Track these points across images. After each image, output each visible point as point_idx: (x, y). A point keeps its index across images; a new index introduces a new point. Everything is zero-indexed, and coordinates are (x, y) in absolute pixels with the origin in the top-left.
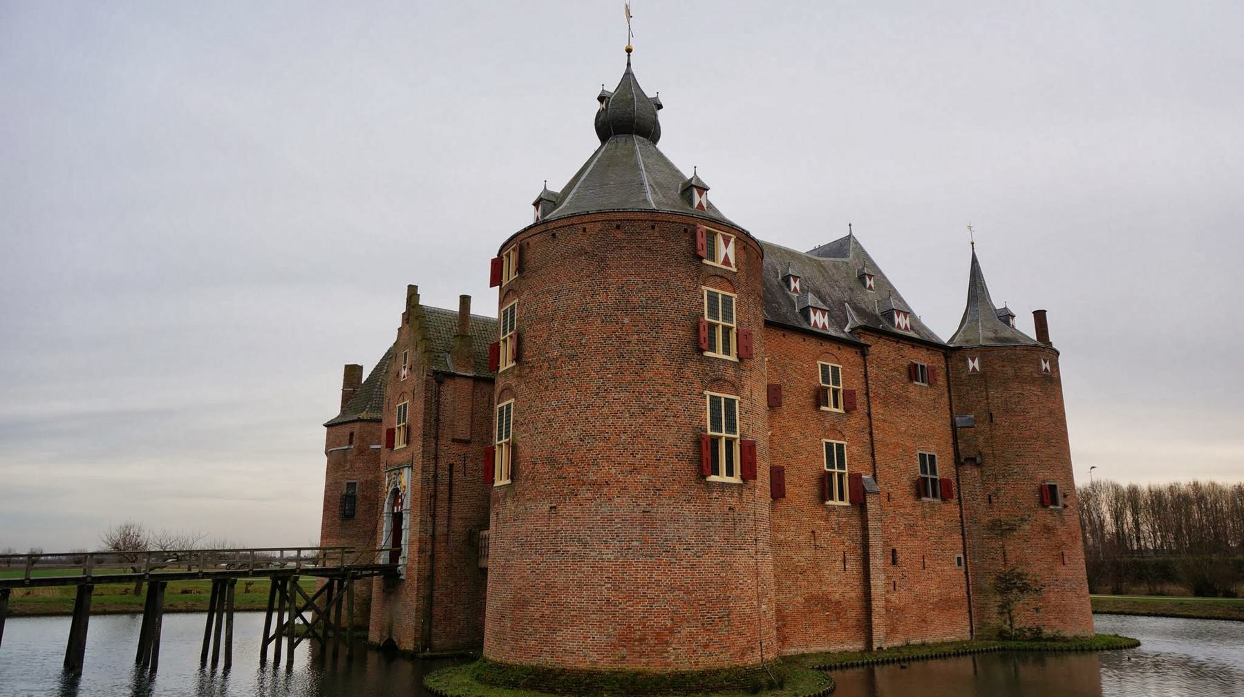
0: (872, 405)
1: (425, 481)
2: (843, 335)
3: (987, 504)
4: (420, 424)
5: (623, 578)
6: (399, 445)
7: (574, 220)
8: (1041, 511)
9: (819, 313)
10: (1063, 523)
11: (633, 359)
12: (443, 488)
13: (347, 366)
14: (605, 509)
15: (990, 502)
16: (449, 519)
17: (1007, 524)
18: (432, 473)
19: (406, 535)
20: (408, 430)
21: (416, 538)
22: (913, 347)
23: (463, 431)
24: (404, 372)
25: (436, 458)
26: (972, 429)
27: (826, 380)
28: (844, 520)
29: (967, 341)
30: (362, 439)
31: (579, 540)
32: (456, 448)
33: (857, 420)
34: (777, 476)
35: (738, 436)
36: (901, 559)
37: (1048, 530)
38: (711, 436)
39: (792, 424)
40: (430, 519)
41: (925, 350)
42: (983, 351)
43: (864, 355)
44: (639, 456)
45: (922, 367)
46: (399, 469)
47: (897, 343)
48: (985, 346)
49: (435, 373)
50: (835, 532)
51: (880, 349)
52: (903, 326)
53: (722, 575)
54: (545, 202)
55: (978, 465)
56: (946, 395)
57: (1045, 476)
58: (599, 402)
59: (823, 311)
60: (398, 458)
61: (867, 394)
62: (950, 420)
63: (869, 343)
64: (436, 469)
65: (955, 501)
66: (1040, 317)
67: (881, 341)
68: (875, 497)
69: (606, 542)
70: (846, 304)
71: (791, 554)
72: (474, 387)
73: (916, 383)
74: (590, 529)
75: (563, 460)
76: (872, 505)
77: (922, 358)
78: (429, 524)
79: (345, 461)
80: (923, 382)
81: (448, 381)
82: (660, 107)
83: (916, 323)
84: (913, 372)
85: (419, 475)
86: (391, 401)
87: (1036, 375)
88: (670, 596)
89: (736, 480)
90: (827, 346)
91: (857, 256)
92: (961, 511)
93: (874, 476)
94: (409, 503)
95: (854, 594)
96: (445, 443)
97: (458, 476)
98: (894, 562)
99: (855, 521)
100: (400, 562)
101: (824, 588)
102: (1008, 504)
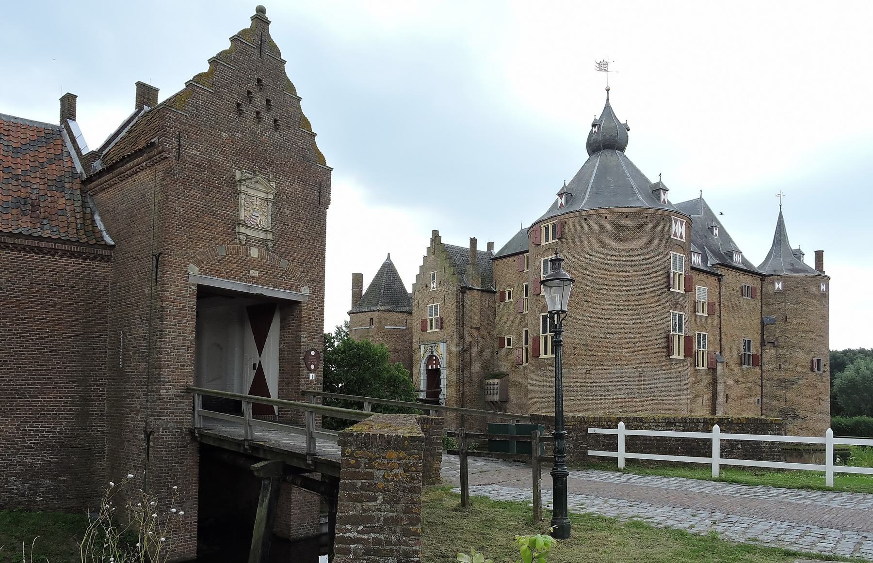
1: (458, 352)
7: (600, 211)
11: (634, 293)
12: (467, 355)
15: (780, 369)
16: (471, 373)
18: (462, 347)
19: (443, 383)
23: (476, 322)
24: (433, 286)
28: (704, 377)
30: (380, 322)
32: (473, 333)
40: (461, 373)
46: (436, 343)
49: (462, 287)
54: (567, 194)
57: (815, 355)
58: (616, 316)
60: (432, 337)
64: (463, 344)
65: (759, 367)
76: (720, 369)
78: (461, 376)
79: (368, 336)
81: (468, 292)
85: (454, 348)
92: (762, 373)
93: (720, 352)
94: (445, 364)
97: (474, 349)
99: (710, 378)
100: (441, 397)
102: (791, 370)
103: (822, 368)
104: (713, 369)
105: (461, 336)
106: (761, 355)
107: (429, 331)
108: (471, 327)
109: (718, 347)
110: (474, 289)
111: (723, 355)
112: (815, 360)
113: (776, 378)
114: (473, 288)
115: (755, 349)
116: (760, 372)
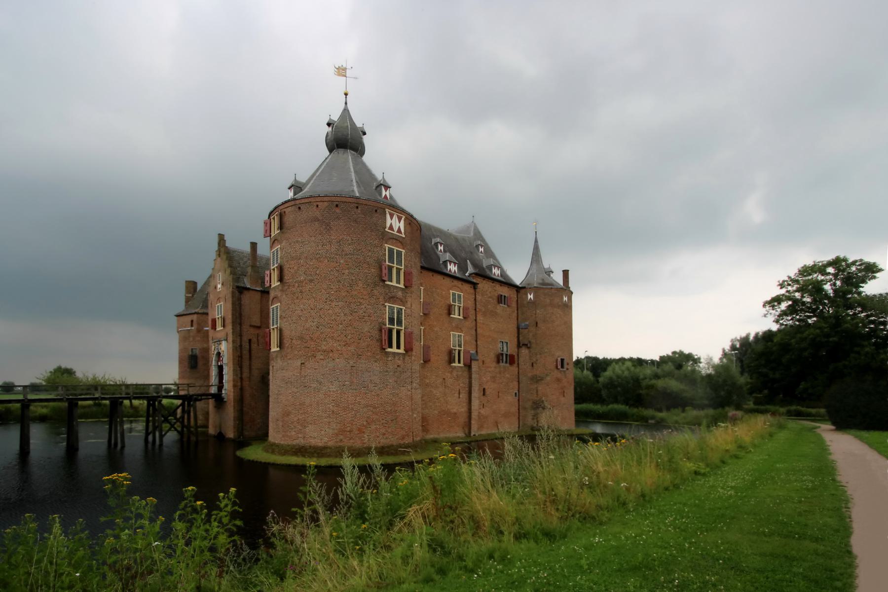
0: (477, 315)
2: (464, 277)
3: (531, 367)
4: (230, 316)
5: (341, 400)
6: (219, 328)
8: (556, 371)
9: (452, 264)
13: (186, 282)
14: (331, 365)
17: (540, 377)
20: (224, 320)
22: (501, 285)
25: (241, 336)
26: (527, 330)
27: (454, 301)
28: (460, 373)
29: (528, 284)
31: (317, 381)
32: (252, 330)
33: (470, 323)
34: (426, 349)
35: (403, 328)
36: (487, 392)
37: (558, 380)
38: (389, 328)
39: (435, 323)
41: (507, 288)
42: (535, 290)
43: (475, 288)
44: (349, 337)
45: (505, 296)
47: (493, 283)
48: (537, 287)
50: (455, 379)
51: (483, 285)
52: (497, 275)
53: (393, 399)
55: (529, 348)
56: (516, 311)
59: (455, 263)
61: (475, 310)
62: (516, 325)
63: (478, 282)
66: (566, 273)
67: (484, 282)
69: (332, 382)
70: (468, 261)
71: (431, 389)
72: (261, 297)
73: (501, 305)
74: (323, 375)
75: (308, 338)
76: (475, 366)
77: (505, 291)
80: (504, 304)
81: (246, 292)
83: (503, 274)
84: (501, 299)
86: (213, 303)
87: (560, 303)
88: (365, 410)
89: (402, 351)
90: (456, 282)
91: (475, 234)
93: (477, 351)
95: (464, 409)
96: (245, 327)
98: (484, 394)
99: (466, 374)
101: (448, 406)
103: (565, 366)
104: (469, 366)
105: (238, 334)
106: (518, 355)
107: (218, 329)
108: (251, 326)
109: (474, 346)
110: (253, 290)
111: (479, 354)
112: (559, 359)
113: (530, 375)
114: (252, 288)
115: (512, 349)
116: (517, 369)
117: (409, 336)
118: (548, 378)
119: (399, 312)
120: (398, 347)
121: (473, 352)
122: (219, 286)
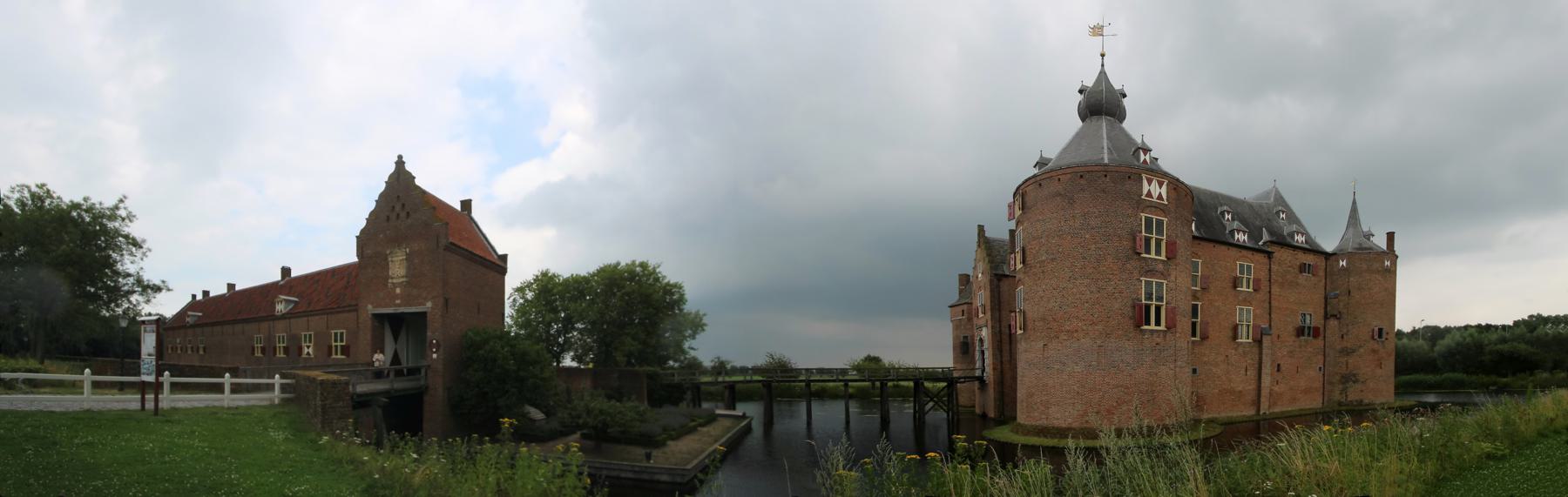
8: (1372, 342)
10: (1384, 347)
18: (998, 329)
21: (991, 362)
25: (1000, 321)
37: (1374, 351)
46: (980, 328)
55: (1338, 319)
64: (1000, 327)
68: (1269, 337)
76: (1266, 341)
78: (999, 356)
82: (1124, 96)
89: (1162, 327)
93: (1270, 325)
99: (1255, 350)
104: (1258, 342)
115: (1315, 319)
117: (1172, 313)
118: (1362, 350)
119: (1160, 285)
120: (1158, 323)
121: (1267, 326)
122: (980, 275)
